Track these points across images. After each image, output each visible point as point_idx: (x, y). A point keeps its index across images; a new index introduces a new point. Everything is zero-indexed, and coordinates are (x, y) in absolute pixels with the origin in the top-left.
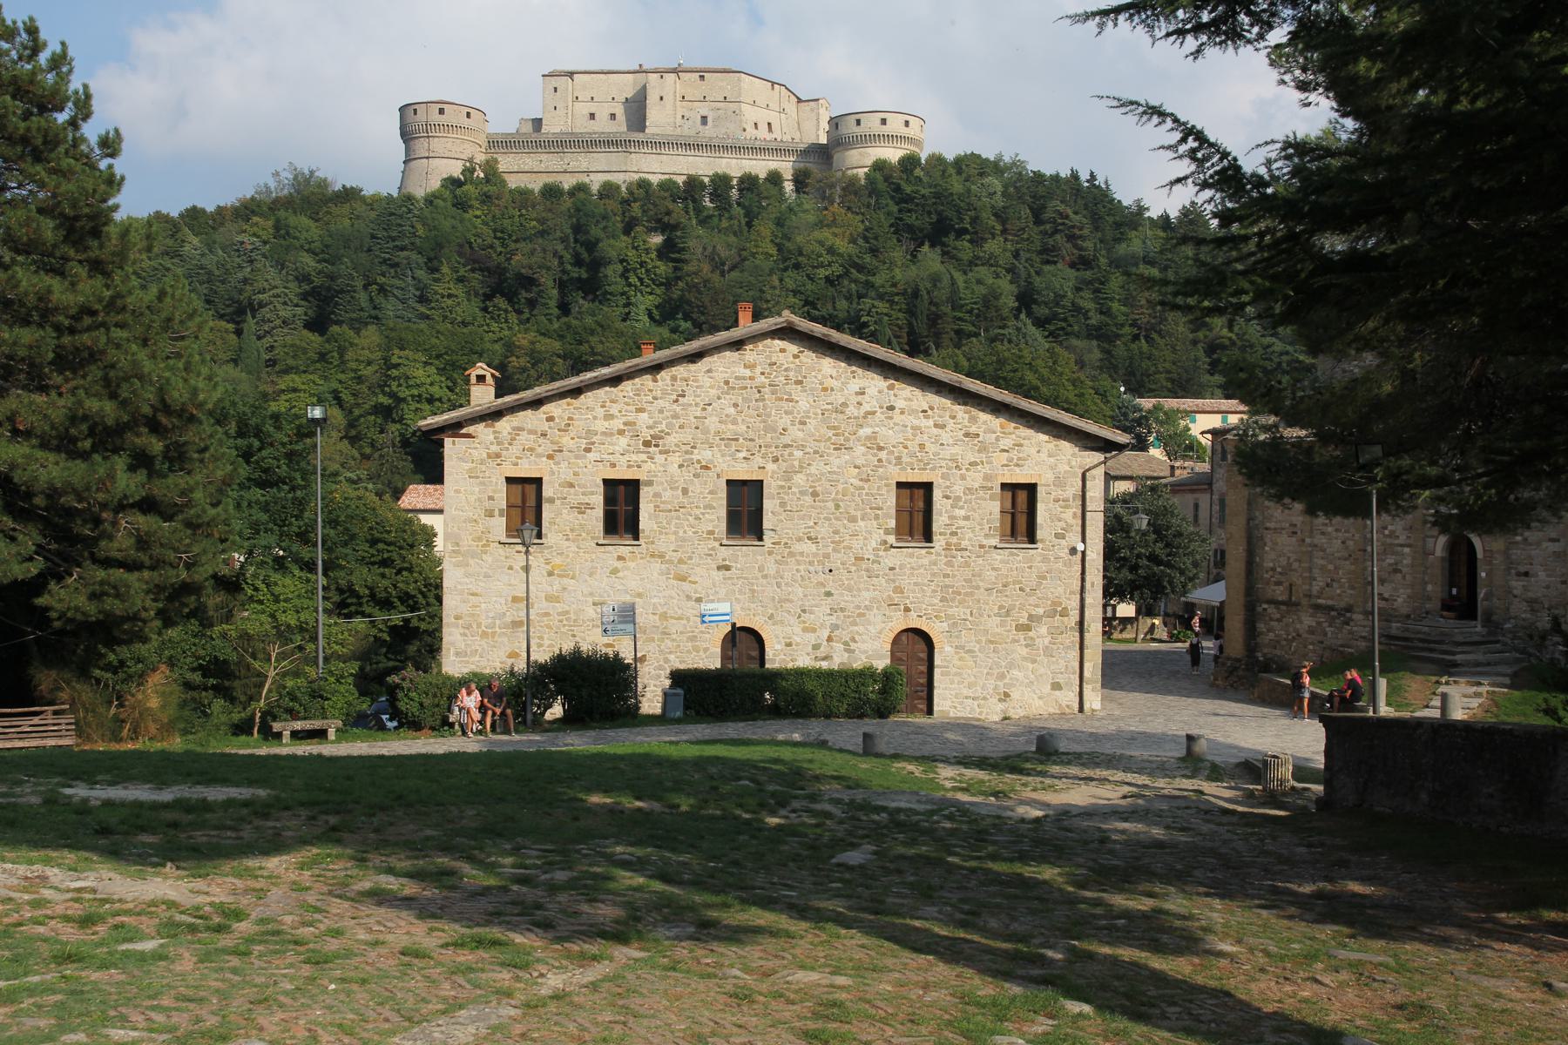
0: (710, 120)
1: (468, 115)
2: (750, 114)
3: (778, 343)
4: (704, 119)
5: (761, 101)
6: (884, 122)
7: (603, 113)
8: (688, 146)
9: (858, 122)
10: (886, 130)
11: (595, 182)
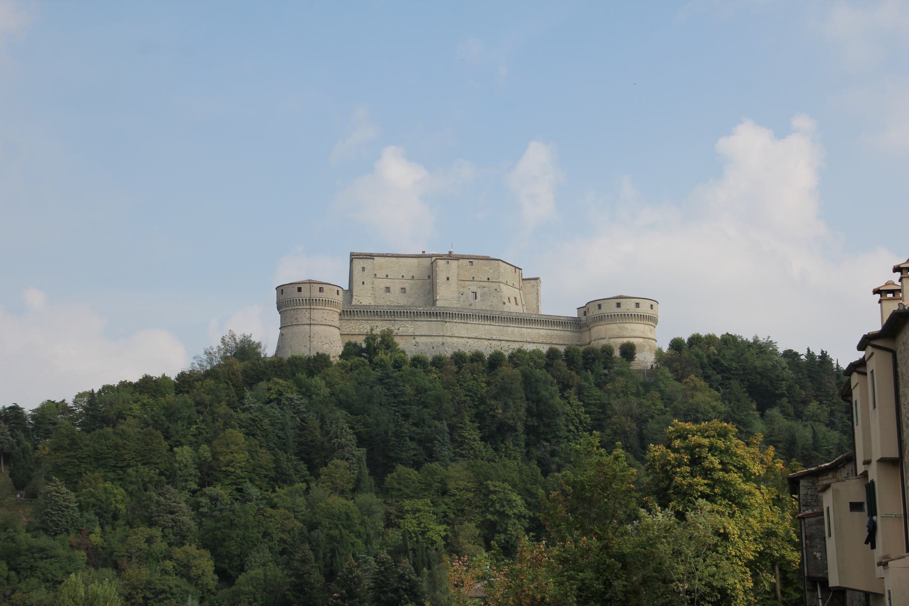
0: (478, 295)
5: (509, 283)
6: (637, 305)
7: (396, 287)
8: (486, 318)
9: (619, 305)
10: (639, 311)
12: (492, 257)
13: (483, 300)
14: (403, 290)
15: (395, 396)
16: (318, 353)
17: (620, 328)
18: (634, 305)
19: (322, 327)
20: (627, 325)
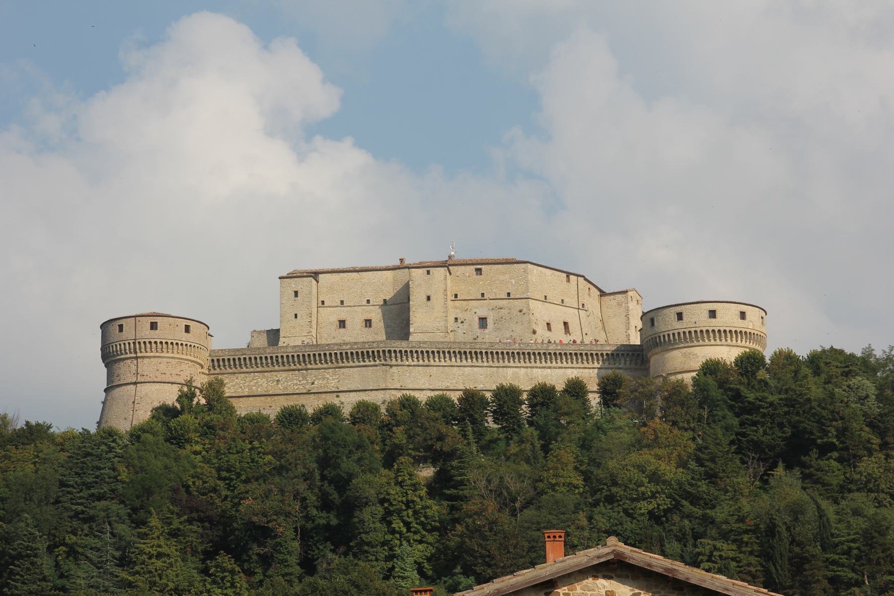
0: (490, 322)
1: (187, 329)
2: (540, 312)
3: (604, 584)
4: (483, 322)
6: (713, 314)
8: (463, 354)
9: (680, 316)
10: (717, 324)
11: (347, 403)
12: (518, 259)
13: (497, 329)
14: (368, 323)
15: (89, 486)
16: (27, 423)
17: (685, 355)
18: (707, 314)
19: (157, 386)
20: (696, 350)
